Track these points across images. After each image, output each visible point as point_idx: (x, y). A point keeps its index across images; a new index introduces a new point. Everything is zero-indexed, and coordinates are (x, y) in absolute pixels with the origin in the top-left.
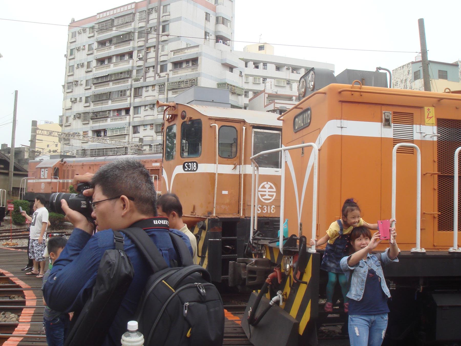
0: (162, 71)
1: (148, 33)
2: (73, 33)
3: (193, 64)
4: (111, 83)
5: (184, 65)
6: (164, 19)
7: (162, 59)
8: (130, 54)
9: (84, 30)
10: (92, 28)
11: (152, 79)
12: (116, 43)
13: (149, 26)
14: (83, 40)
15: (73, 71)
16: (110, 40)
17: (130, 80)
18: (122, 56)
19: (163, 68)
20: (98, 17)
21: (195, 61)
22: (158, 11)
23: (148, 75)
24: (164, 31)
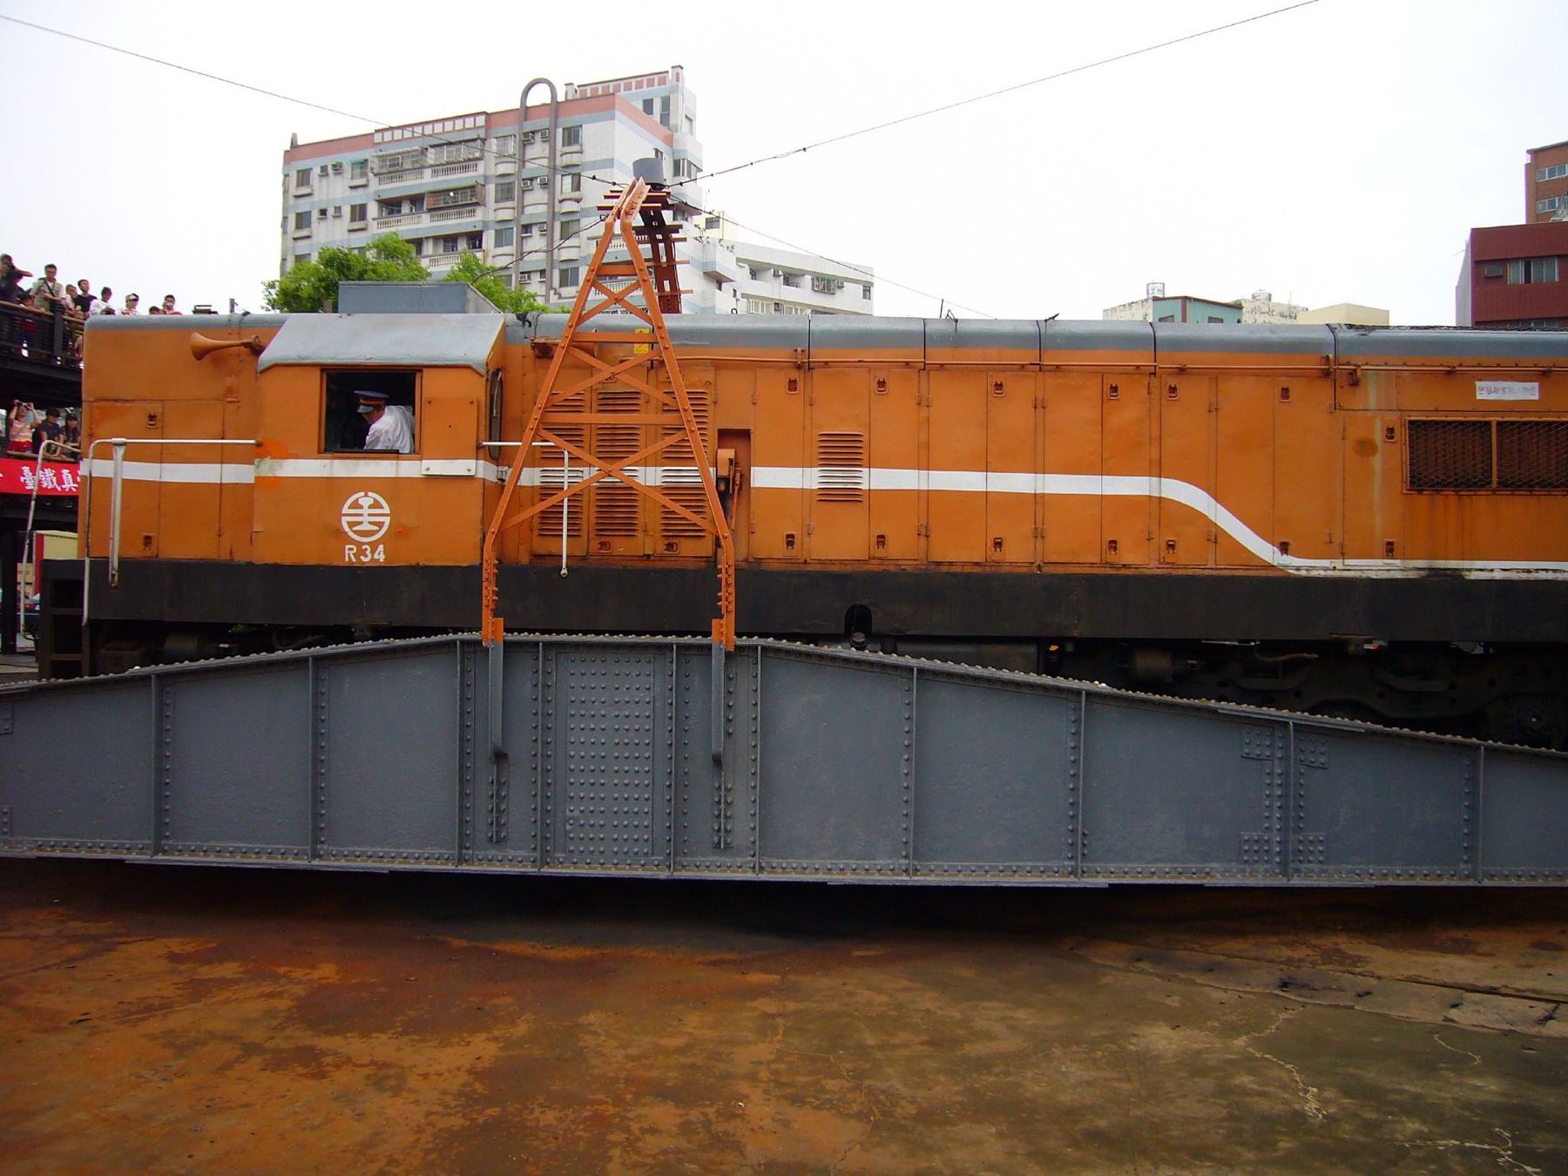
0: (563, 283)
6: (567, 160)
7: (565, 254)
8: (475, 239)
12: (430, 210)
14: (335, 191)
16: (416, 200)
20: (378, 138)
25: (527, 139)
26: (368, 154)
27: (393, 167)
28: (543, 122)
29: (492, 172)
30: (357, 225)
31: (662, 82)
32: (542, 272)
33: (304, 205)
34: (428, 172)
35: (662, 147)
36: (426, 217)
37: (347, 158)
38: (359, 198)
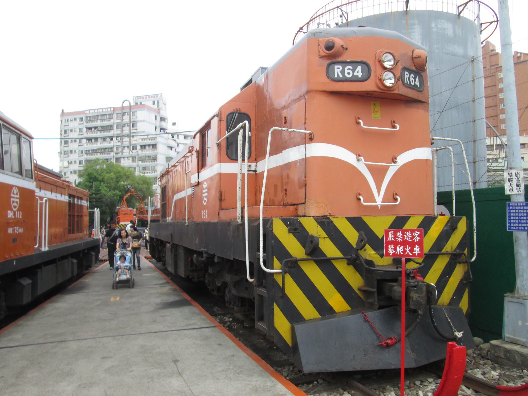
0: (133, 149)
1: (123, 127)
2: (65, 120)
3: (153, 147)
4: (99, 154)
5: (147, 147)
6: (133, 120)
7: (133, 143)
9: (75, 119)
10: (82, 119)
11: (127, 154)
13: (123, 123)
14: (75, 125)
15: (68, 143)
16: (96, 128)
17: (112, 153)
18: (104, 139)
19: (134, 148)
21: (154, 146)
22: (129, 114)
23: (124, 151)
24: (133, 127)
25: (124, 114)
26: (84, 116)
27: (90, 119)
28: (128, 110)
29: (115, 121)
30: (81, 133)
31: (157, 97)
32: (128, 147)
33: (66, 128)
34: (99, 121)
35: (157, 114)
36: (99, 132)
37: (78, 117)
38: (81, 126)
